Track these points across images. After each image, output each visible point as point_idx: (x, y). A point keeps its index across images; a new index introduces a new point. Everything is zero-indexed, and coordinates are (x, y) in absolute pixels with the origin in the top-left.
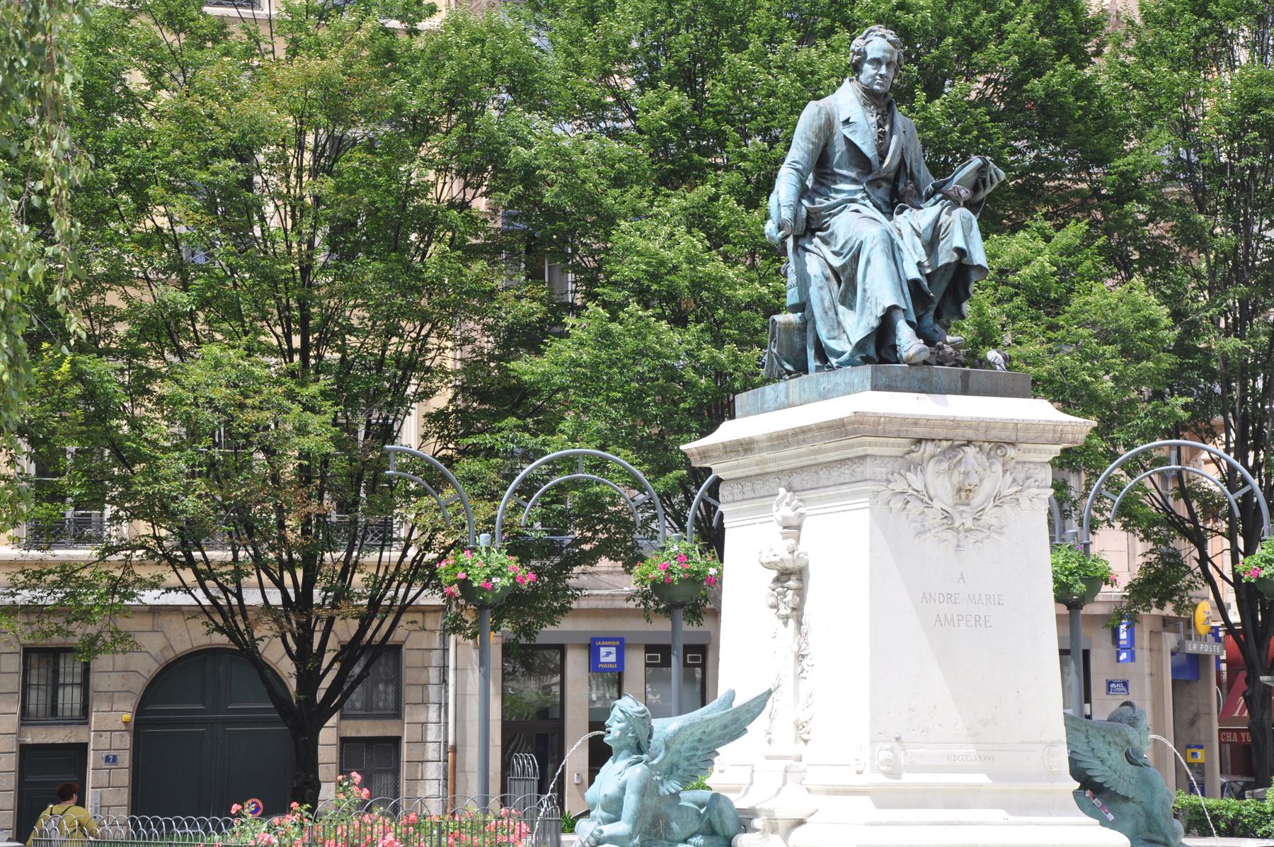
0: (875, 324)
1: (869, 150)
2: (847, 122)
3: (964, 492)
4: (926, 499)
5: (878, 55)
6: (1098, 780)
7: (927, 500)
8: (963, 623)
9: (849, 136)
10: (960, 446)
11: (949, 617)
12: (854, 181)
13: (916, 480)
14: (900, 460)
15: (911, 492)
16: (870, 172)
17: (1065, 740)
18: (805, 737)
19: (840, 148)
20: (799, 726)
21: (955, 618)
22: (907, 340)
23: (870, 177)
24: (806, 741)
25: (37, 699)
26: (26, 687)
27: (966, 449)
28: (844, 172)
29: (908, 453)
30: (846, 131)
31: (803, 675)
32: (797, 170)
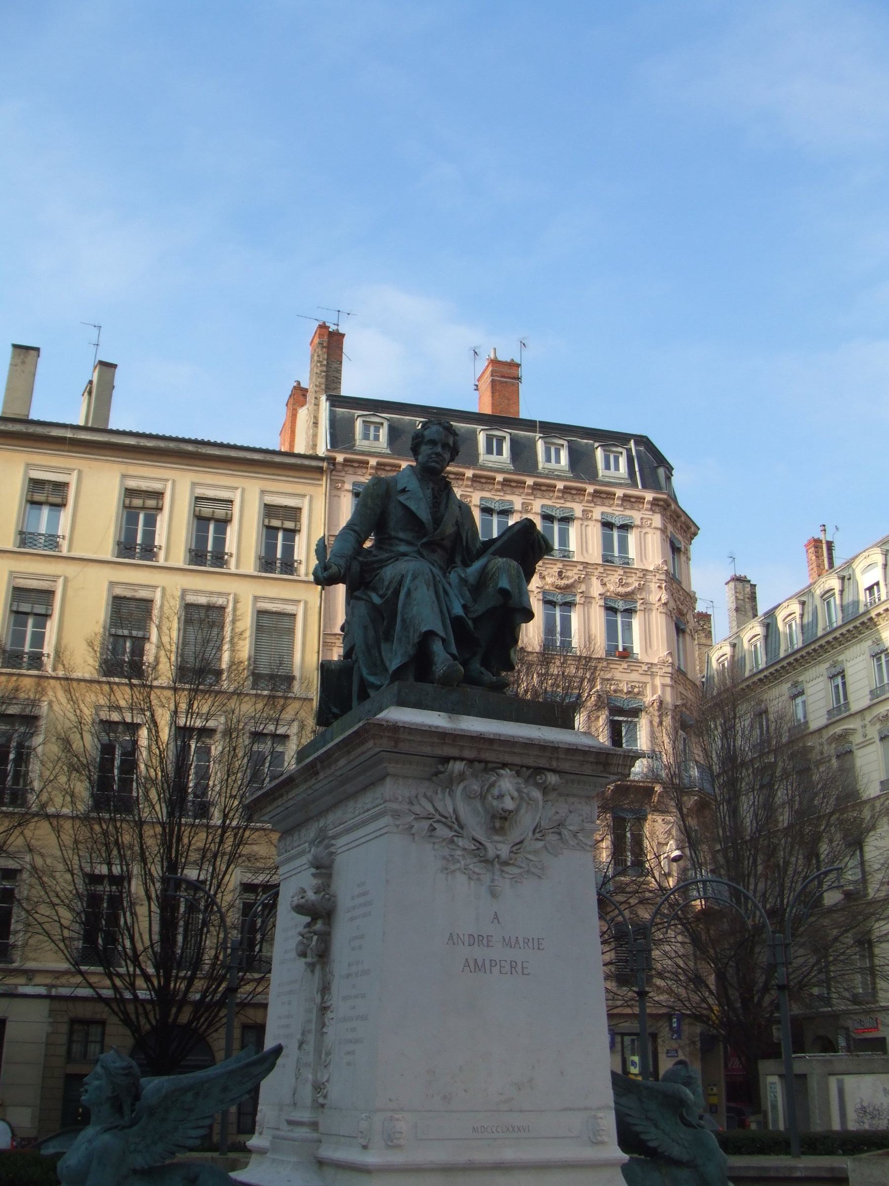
0: (411, 651)
1: (423, 512)
2: (404, 491)
3: (500, 821)
4: (456, 826)
5: (435, 437)
6: (652, 1144)
7: (457, 825)
8: (496, 970)
9: (407, 503)
10: (493, 769)
11: (480, 962)
12: (409, 543)
13: (446, 805)
14: (427, 783)
15: (438, 817)
16: (425, 535)
17: (612, 1104)
18: (321, 1100)
19: (395, 513)
20: (318, 1087)
21: (487, 963)
22: (442, 658)
23: (424, 540)
24: (323, 1106)
25: (76, 1048)
26: (70, 1042)
27: (502, 772)
28: (401, 535)
29: (436, 774)
30: (402, 498)
31: (325, 1030)
32: (354, 531)
